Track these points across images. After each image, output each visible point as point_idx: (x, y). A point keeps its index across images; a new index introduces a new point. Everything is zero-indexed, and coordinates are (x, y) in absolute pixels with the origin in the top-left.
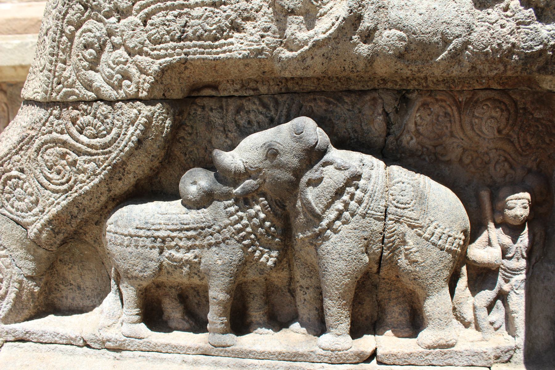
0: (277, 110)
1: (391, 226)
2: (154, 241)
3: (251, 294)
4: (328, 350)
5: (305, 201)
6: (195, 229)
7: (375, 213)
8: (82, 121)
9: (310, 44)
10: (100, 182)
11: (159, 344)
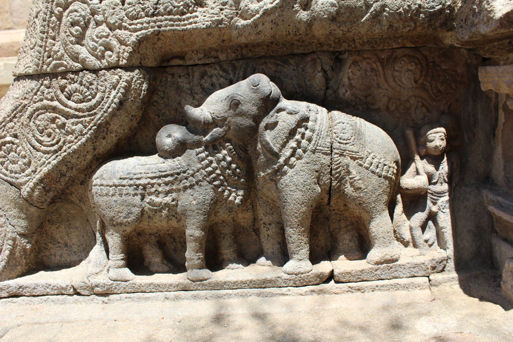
0: (235, 74)
1: (336, 159)
2: (136, 189)
3: (221, 233)
4: (292, 274)
5: (264, 143)
6: (172, 175)
7: (322, 149)
8: (70, 89)
9: (261, 12)
10: (87, 141)
11: (143, 284)
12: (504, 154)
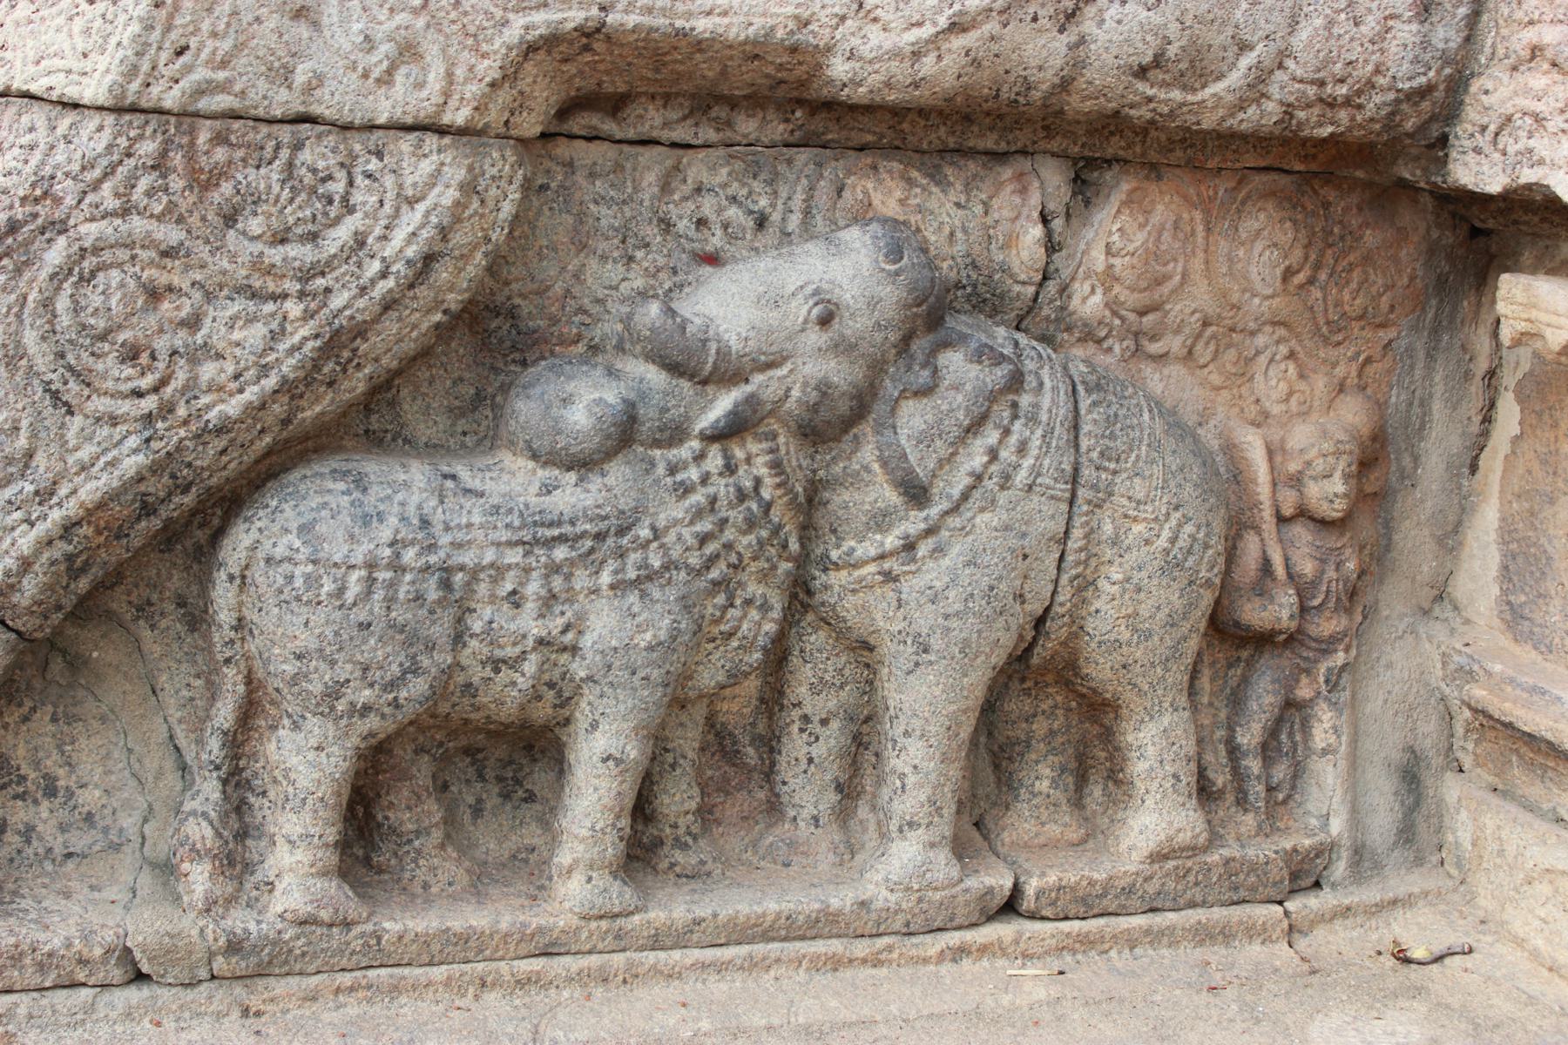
3: (667, 750)
9: (943, 22)
12: (1507, 532)
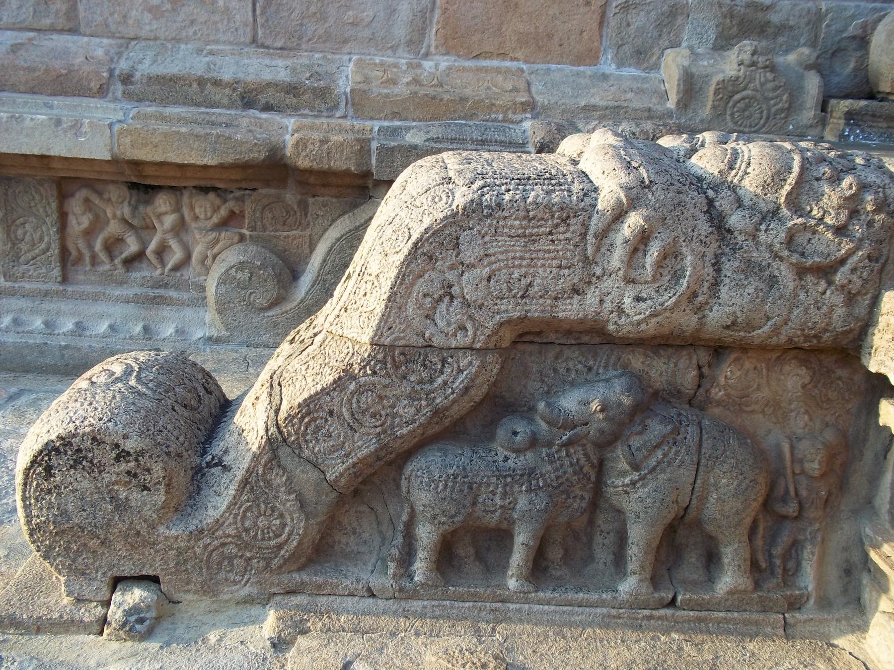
0: (596, 360)
9: (647, 313)
